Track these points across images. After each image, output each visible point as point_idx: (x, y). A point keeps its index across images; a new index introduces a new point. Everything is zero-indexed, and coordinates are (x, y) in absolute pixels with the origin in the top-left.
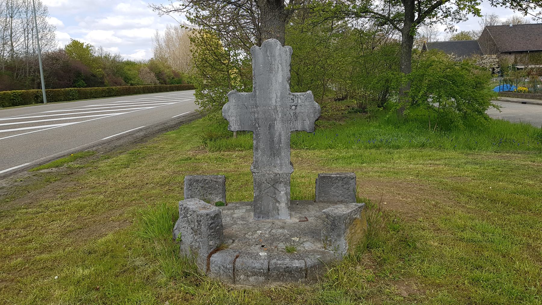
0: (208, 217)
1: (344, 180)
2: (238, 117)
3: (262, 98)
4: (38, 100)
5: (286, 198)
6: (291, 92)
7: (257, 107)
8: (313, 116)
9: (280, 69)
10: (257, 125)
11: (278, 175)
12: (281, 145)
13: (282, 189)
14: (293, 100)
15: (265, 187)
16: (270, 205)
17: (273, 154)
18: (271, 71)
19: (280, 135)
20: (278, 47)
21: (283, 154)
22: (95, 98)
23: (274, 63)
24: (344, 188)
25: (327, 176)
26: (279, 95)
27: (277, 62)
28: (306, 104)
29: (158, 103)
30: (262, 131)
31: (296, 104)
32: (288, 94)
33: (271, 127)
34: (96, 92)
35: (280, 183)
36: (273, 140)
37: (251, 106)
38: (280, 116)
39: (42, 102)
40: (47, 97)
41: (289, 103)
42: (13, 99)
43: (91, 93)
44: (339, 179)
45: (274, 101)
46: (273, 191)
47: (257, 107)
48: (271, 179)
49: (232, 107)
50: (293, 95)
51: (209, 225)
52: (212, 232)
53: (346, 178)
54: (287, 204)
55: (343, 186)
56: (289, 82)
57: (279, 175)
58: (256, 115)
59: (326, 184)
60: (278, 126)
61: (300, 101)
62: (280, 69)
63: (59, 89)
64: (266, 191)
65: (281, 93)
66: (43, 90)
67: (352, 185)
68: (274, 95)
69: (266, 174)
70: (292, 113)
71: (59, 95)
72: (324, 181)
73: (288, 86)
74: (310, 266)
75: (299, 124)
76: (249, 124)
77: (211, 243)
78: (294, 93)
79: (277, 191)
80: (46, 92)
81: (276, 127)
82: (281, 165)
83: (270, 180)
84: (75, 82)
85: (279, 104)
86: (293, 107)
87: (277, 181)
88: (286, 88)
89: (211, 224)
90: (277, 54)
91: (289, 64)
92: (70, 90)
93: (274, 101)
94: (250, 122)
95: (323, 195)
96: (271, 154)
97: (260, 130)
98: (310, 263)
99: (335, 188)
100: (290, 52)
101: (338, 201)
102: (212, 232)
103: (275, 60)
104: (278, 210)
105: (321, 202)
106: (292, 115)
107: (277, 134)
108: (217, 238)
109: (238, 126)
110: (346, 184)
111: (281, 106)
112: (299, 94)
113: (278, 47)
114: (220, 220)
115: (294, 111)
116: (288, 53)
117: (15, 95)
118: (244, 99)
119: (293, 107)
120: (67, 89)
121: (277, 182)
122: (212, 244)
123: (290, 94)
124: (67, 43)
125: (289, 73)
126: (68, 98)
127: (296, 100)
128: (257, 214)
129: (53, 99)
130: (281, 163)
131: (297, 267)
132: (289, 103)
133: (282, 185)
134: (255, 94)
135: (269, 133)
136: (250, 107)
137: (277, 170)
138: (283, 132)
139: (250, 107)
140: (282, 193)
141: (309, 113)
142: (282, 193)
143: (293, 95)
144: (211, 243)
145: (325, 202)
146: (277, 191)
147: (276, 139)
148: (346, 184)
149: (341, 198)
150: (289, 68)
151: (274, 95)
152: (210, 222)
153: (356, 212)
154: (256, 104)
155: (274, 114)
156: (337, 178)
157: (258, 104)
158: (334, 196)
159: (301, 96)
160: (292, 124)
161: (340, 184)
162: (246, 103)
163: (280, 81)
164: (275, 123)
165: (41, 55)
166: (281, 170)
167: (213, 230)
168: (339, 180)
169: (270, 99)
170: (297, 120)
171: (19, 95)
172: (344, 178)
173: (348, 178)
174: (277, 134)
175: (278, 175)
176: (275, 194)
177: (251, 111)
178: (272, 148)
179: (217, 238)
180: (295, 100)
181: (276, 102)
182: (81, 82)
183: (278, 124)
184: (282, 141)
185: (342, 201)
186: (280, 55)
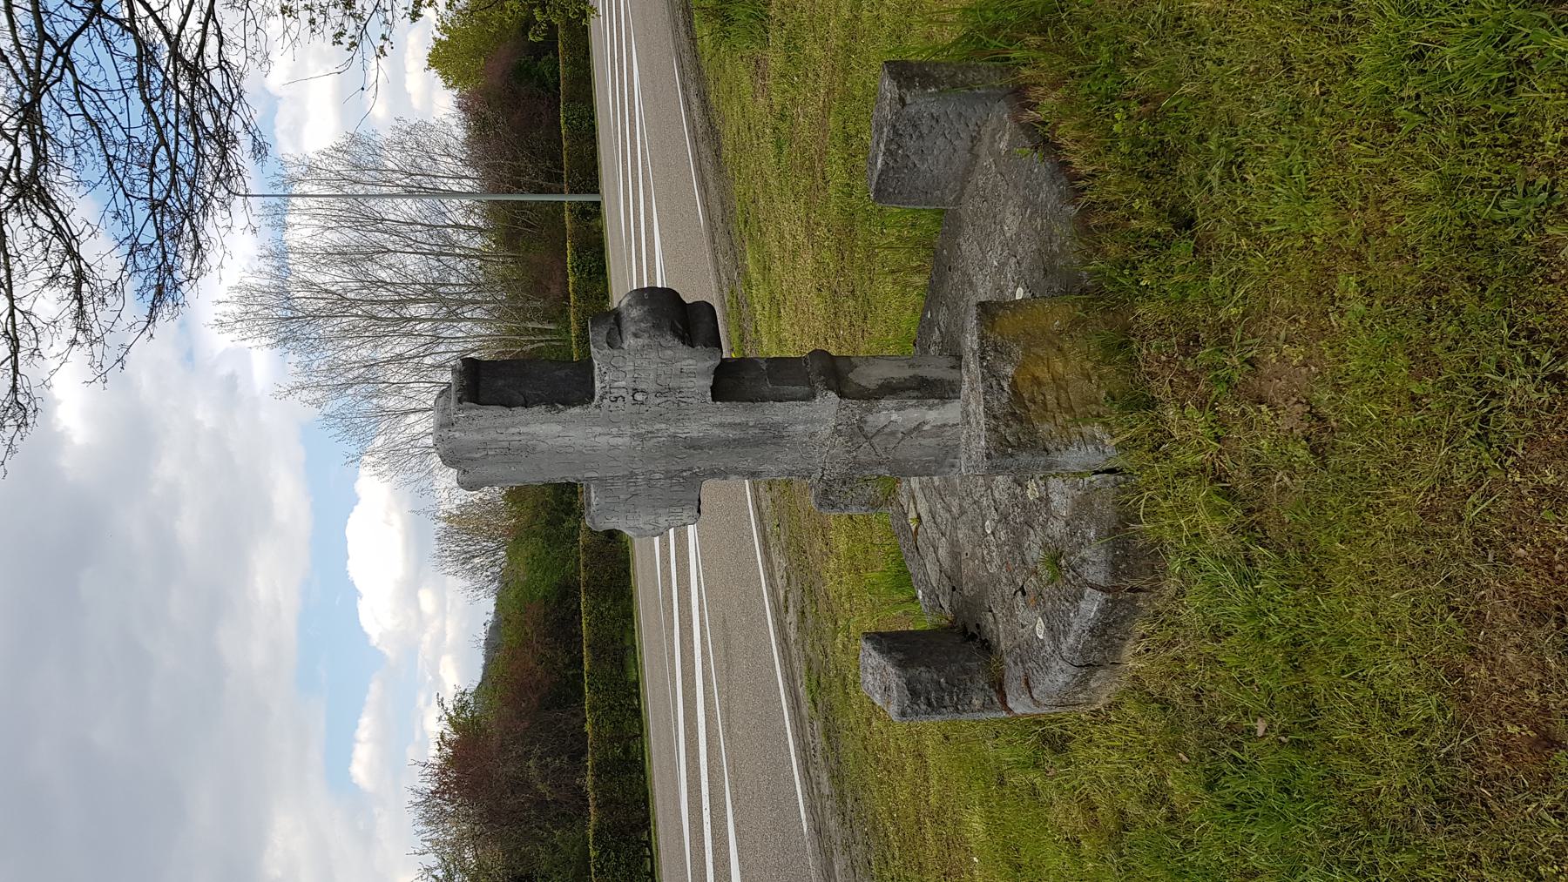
0: (909, 711)
1: (901, 132)
2: (660, 511)
3: (610, 464)
4: (591, 213)
5: (912, 410)
6: (593, 404)
7: (632, 475)
8: (669, 352)
9: (523, 429)
10: (685, 474)
11: (839, 428)
12: (751, 424)
13: (882, 419)
14: (617, 398)
15: (869, 454)
16: (922, 442)
17: (775, 440)
18: (529, 450)
19: (721, 425)
20: (457, 435)
21: (779, 419)
22: (588, 53)
23: (505, 444)
24: (930, 132)
25: (877, 183)
26: (598, 430)
27: (502, 437)
28: (632, 368)
29: (612, 35)
30: (700, 462)
31: (631, 392)
32: (598, 410)
33: (694, 445)
34: (569, 48)
35: (866, 422)
36: (735, 440)
37: (628, 487)
38: (663, 426)
39: (598, 204)
40: (589, 192)
41: (625, 408)
42: (589, 273)
43: (575, 63)
44: (893, 147)
45: (619, 441)
46: (885, 437)
47: (632, 475)
48: (847, 442)
49: (631, 524)
50: (602, 398)
51: (930, 710)
52: (951, 699)
53: (895, 126)
54: (930, 408)
55: (921, 136)
56: (561, 407)
57: (840, 424)
58: (657, 476)
59: (903, 184)
60: (693, 429)
61: (623, 384)
62: (523, 429)
63: (565, 153)
64: (880, 451)
65: (594, 425)
66: (567, 198)
67: (926, 107)
68: (602, 440)
69: (831, 452)
70: (658, 401)
71: (581, 157)
72: (891, 190)
73: (576, 410)
74: (1110, 579)
75: (690, 385)
76: (683, 489)
77: (977, 703)
78: (597, 398)
79: (887, 430)
80: (573, 191)
81: (695, 434)
82: (812, 421)
83: (850, 444)
84: (542, 83)
85: (627, 429)
86: (639, 397)
87: (857, 430)
88: (581, 414)
89: (929, 704)
90: (477, 437)
91: (508, 410)
92: (566, 123)
93: (619, 441)
94: (676, 488)
95: (938, 192)
96: (774, 444)
97: (699, 468)
98: (1102, 576)
99: (923, 160)
100: (471, 408)
101: (971, 150)
102: (951, 699)
103: (497, 441)
104: (945, 425)
105: (960, 198)
106: (664, 399)
107: (717, 431)
108: (969, 684)
109: (685, 512)
110: (915, 126)
111: (633, 424)
112: (597, 384)
113: (457, 435)
114: (923, 674)
115: (652, 396)
116: (474, 412)
117: (580, 267)
118: (608, 500)
119: (639, 397)
120: (563, 132)
121: (860, 428)
122: (982, 701)
123: (598, 407)
124: (439, 81)
125: (536, 409)
126: (587, 134)
127: (616, 393)
128: (942, 470)
129: (588, 177)
130: (806, 422)
131: (1100, 610)
132: (625, 408)
133: (870, 418)
134: (597, 479)
135: (711, 449)
136: (632, 489)
137: (825, 431)
138: (712, 420)
139: (632, 489)
140: (894, 417)
141: (659, 360)
142: (894, 417)
143: (602, 398)
144: (977, 703)
145: (963, 188)
146: (887, 430)
147: (732, 434)
148: (915, 126)
149: (962, 144)
150: (519, 410)
151: (602, 440)
152: (923, 707)
153: (994, 383)
154: (623, 476)
155: (655, 440)
156: (891, 154)
157: (626, 473)
158: (949, 161)
159: (607, 378)
160: (690, 400)
161: (911, 144)
162: (622, 497)
163: (560, 428)
164: (685, 435)
165: (481, 194)
166: (823, 421)
167: (947, 697)
168: (898, 149)
169: (616, 447)
170: (679, 388)
171: (579, 257)
172: (896, 132)
173: (897, 120)
174: (717, 431)
175: (839, 428)
176: (893, 433)
177: (646, 487)
178: (757, 443)
179: (969, 684)
180: (616, 395)
181: (619, 436)
182: (543, 66)
183: (686, 431)
184: (738, 421)
185: (973, 139)
186: (479, 430)
